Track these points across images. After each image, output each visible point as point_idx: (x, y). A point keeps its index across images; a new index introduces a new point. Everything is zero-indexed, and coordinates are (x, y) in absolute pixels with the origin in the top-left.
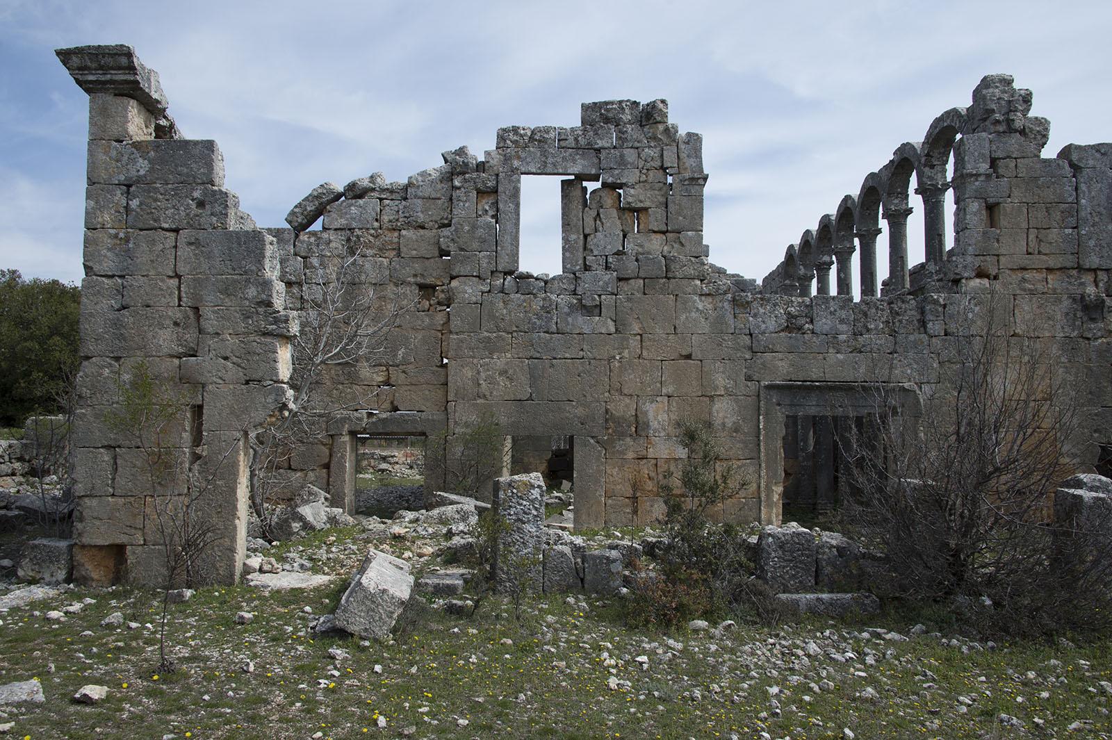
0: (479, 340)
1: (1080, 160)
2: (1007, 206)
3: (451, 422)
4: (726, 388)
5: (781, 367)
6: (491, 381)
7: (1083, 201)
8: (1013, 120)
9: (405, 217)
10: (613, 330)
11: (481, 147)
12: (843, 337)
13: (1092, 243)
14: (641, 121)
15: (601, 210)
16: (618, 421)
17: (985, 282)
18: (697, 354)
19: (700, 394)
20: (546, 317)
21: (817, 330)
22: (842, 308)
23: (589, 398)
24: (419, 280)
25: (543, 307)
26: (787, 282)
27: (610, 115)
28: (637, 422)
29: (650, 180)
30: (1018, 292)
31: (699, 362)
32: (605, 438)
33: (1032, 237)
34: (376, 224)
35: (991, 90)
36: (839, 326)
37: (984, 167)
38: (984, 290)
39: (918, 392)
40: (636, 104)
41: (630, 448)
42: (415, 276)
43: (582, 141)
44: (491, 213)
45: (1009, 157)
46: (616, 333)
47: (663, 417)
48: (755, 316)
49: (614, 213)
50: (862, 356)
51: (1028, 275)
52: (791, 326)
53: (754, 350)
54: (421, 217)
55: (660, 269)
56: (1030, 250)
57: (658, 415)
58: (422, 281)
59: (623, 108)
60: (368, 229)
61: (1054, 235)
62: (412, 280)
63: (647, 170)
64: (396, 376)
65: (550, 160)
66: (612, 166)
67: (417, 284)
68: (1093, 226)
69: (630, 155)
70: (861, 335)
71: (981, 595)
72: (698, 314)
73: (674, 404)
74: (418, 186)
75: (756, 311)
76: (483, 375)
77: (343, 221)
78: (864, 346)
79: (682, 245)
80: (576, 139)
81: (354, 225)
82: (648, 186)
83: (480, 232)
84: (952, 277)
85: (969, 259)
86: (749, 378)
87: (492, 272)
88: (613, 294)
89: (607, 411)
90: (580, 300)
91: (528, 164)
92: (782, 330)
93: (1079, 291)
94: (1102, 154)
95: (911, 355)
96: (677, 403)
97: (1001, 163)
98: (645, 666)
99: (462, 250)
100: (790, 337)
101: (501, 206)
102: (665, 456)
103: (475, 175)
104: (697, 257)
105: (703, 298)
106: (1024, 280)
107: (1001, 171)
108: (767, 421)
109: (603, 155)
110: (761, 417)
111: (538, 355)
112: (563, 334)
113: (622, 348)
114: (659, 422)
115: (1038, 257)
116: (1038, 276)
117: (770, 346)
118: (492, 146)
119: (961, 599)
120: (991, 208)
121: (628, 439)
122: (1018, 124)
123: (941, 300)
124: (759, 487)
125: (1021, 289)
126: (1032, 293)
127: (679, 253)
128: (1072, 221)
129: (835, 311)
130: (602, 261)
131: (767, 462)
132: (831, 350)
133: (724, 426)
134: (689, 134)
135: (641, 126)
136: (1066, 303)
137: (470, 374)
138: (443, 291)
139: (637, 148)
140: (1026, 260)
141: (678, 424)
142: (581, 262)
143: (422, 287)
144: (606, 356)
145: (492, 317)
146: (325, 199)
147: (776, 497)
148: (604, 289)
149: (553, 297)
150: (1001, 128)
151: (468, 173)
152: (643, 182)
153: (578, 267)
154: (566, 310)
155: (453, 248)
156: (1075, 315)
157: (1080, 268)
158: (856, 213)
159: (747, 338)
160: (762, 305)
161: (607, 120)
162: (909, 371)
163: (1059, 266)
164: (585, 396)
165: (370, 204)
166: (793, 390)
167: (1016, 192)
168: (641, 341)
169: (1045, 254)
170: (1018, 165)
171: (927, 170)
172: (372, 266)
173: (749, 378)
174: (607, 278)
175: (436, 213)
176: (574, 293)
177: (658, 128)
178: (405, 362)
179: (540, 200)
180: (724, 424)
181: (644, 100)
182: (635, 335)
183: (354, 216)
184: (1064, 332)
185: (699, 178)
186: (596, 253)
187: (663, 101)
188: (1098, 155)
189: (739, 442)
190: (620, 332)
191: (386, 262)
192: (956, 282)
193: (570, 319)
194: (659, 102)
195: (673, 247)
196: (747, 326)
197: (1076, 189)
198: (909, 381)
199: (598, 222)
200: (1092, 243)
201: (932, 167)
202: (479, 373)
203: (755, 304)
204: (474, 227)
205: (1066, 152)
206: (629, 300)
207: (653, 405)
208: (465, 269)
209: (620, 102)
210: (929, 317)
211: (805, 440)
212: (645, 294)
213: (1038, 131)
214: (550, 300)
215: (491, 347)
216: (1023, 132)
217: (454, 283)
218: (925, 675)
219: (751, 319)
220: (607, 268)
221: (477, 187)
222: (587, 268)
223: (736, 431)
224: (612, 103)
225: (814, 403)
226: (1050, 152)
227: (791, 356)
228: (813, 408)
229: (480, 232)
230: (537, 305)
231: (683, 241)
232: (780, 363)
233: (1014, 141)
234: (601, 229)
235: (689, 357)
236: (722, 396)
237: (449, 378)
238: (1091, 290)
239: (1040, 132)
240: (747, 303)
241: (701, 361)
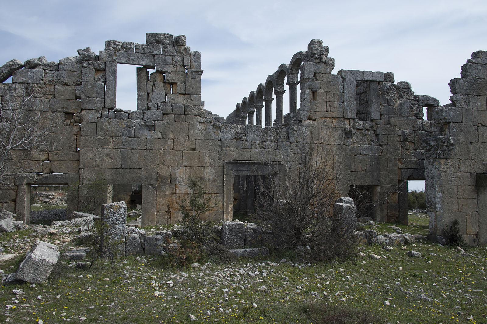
0: (96, 140)
1: (345, 76)
2: (319, 92)
4: (210, 163)
5: (233, 155)
6: (101, 159)
7: (346, 92)
8: (322, 58)
9: (58, 79)
10: (160, 137)
11: (97, 49)
12: (258, 142)
13: (348, 108)
14: (174, 44)
15: (155, 83)
16: (162, 178)
17: (311, 122)
18: (198, 148)
19: (199, 166)
20: (129, 130)
21: (248, 139)
22: (257, 130)
23: (149, 167)
24: (65, 110)
25: (127, 125)
26: (237, 119)
27: (160, 40)
28: (171, 178)
29: (178, 71)
30: (323, 126)
31: (199, 152)
32: (157, 185)
34: (42, 82)
35: (314, 45)
36: (256, 138)
37: (311, 76)
38: (310, 125)
39: (286, 165)
40: (171, 36)
42: (63, 108)
43: (147, 50)
44: (102, 80)
45: (321, 73)
46: (162, 138)
47: (183, 176)
48: (223, 132)
49: (161, 84)
50: (265, 150)
51: (326, 120)
52: (237, 137)
53: (222, 147)
54: (66, 80)
55: (182, 110)
56: (327, 110)
57: (181, 175)
58: (66, 111)
59: (166, 37)
60: (37, 84)
61: (335, 104)
62: (61, 110)
63: (177, 66)
64: (52, 156)
65: (131, 58)
66: (160, 63)
67: (64, 112)
68: (349, 102)
69: (169, 59)
70: (265, 142)
71: (307, 246)
72: (198, 131)
73: (188, 170)
74: (65, 65)
75: (223, 130)
76: (98, 156)
77: (24, 79)
78: (266, 146)
79: (192, 100)
80: (144, 49)
81: (30, 81)
82: (177, 73)
83: (96, 89)
84: (299, 119)
85: (306, 112)
86: (220, 159)
87: (103, 108)
88: (161, 121)
89: (157, 173)
90: (145, 123)
91: (120, 58)
92: (234, 139)
93: (344, 127)
94: (353, 74)
95: (283, 150)
96: (189, 169)
97: (317, 75)
98: (171, 285)
99: (87, 97)
100: (237, 142)
101: (107, 77)
102: (183, 193)
103: (94, 62)
104: (198, 106)
105: (201, 124)
106: (325, 122)
109: (156, 57)
110: (225, 176)
111: (125, 147)
112: (137, 138)
113: (164, 145)
114: (181, 178)
115: (330, 113)
116: (330, 120)
117: (229, 146)
118: (103, 49)
119: (299, 247)
120: (314, 93)
121: (167, 186)
122: (324, 60)
123: (295, 128)
124: (223, 205)
125: (324, 125)
126: (327, 127)
127: (190, 104)
128: (342, 99)
129: (255, 131)
130: (156, 105)
131: (227, 195)
132: (253, 148)
133: (209, 179)
134: (195, 52)
135: (174, 46)
136: (339, 131)
137: (91, 156)
138: (77, 116)
139: (172, 56)
140: (326, 114)
142: (146, 105)
143: (66, 113)
144: (157, 148)
146: (13, 68)
147: (230, 209)
148: (157, 118)
149: (133, 121)
150: (318, 61)
151: (90, 60)
152: (175, 71)
153: (144, 108)
154: (139, 127)
155: (82, 95)
156: (342, 136)
157: (344, 118)
158: (264, 91)
159: (219, 142)
160: (225, 128)
161: (158, 42)
162: (283, 157)
163: (337, 117)
164: (147, 166)
165: (39, 72)
166: (238, 164)
167: (323, 87)
168: (173, 142)
169: (333, 112)
170: (324, 76)
171: (291, 75)
172: (39, 102)
173: (220, 159)
174: (158, 113)
175: (74, 78)
176: (143, 119)
177: (181, 48)
178: (57, 149)
179: (126, 76)
180: (209, 179)
181: (175, 35)
182: (171, 139)
183: (30, 77)
184: (338, 143)
185: (199, 72)
186: (153, 102)
187: (184, 36)
188: (351, 75)
189: (215, 186)
190: (164, 138)
191: (47, 100)
192: (301, 121)
193: (140, 131)
194: (182, 36)
195: (188, 101)
196: (219, 137)
197: (344, 87)
198: (283, 161)
199: (154, 88)
200: (348, 108)
201: (293, 74)
202: (95, 155)
203: (223, 127)
204: (93, 86)
205: (340, 72)
206: (168, 124)
207: (179, 171)
208: (90, 106)
209: (164, 34)
210: (291, 135)
211: (243, 185)
212: (175, 121)
213: (331, 64)
214: (131, 122)
215: (102, 143)
216: (325, 63)
217: (83, 112)
218: (285, 279)
219: (221, 134)
220: (158, 109)
221: (95, 68)
222: (148, 108)
223: (214, 181)
224: (161, 34)
225: (246, 170)
226: (335, 72)
227: (237, 150)
228: (246, 172)
229: (96, 89)
230: (125, 124)
231: (192, 99)
232: (233, 153)
233: (322, 67)
234: (155, 91)
235: (194, 149)
236: (208, 166)
237: (81, 158)
238: (348, 126)
239: (331, 64)
240: (219, 127)
241: (200, 151)
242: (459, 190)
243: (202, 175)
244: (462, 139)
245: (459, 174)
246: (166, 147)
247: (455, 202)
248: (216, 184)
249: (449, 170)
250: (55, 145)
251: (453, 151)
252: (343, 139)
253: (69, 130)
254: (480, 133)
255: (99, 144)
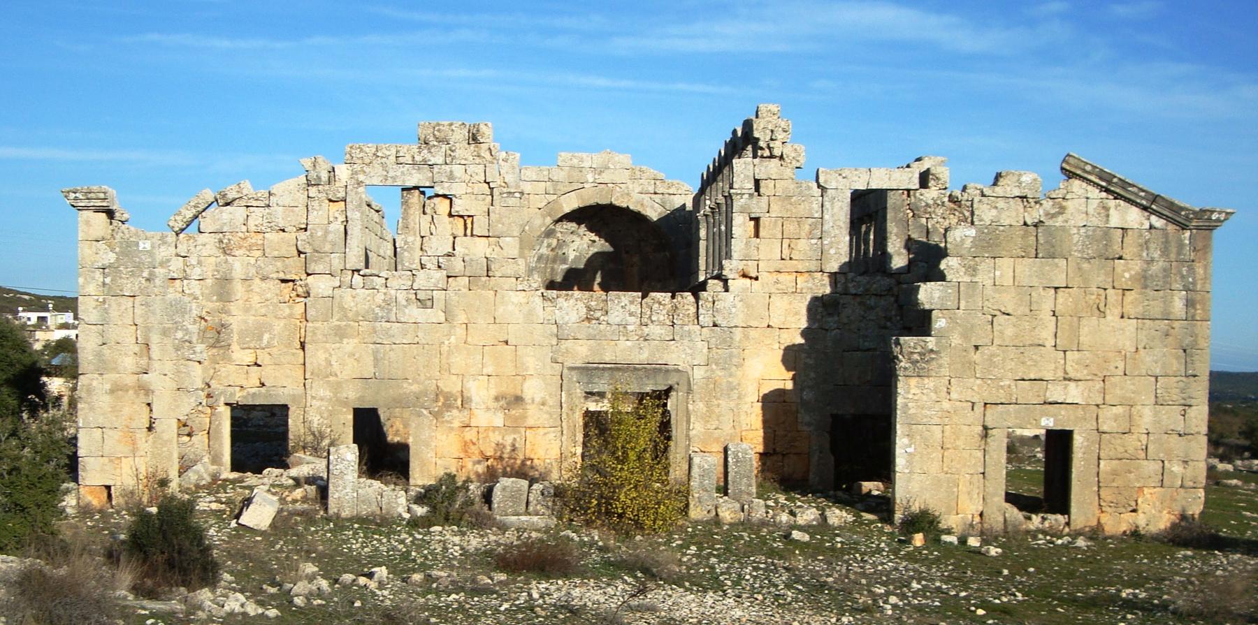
1: (826, 181)
3: (309, 398)
5: (581, 352)
16: (448, 396)
23: (423, 377)
25: (384, 301)
33: (785, 245)
38: (745, 290)
41: (456, 417)
43: (418, 158)
57: (481, 392)
61: (803, 245)
64: (263, 358)
69: (458, 170)
95: (686, 342)
97: (762, 184)
103: (327, 187)
107: (762, 190)
108: (569, 395)
109: (436, 169)
113: (449, 335)
140: (780, 265)
141: (497, 399)
142: (417, 261)
145: (342, 308)
149: (393, 292)
154: (404, 303)
155: (308, 250)
166: (588, 371)
167: (774, 207)
172: (238, 266)
188: (840, 178)
191: (252, 261)
200: (832, 251)
204: (327, 232)
215: (340, 334)
223: (543, 404)
229: (330, 237)
230: (379, 298)
242: (947, 434)
243: (519, 393)
244: (956, 340)
245: (946, 405)
246: (453, 339)
247: (937, 455)
248: (545, 408)
249: (925, 398)
250: (266, 337)
251: (934, 363)
252: (819, 317)
253: (287, 311)
254: (996, 327)
255: (336, 335)
